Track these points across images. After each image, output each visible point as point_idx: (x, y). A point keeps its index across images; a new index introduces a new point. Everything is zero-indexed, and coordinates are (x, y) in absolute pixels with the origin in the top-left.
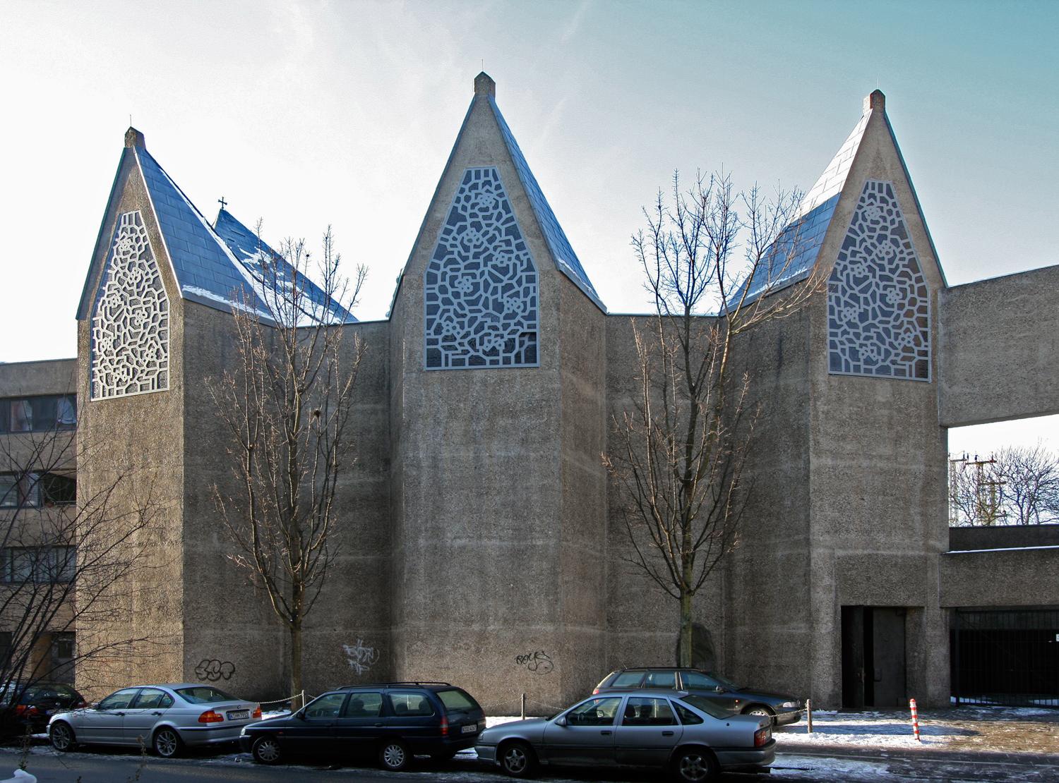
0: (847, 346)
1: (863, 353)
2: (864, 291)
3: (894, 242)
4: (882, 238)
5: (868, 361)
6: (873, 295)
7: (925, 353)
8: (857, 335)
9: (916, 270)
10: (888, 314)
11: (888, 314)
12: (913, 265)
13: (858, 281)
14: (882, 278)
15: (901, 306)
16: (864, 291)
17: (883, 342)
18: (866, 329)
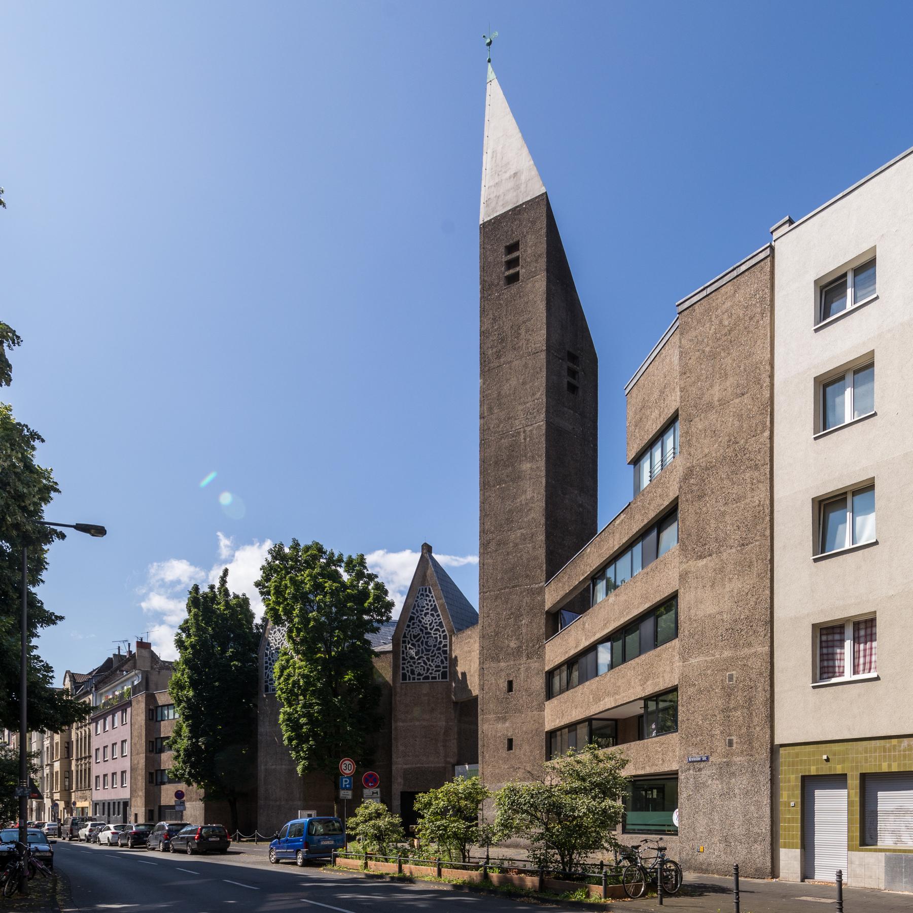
0: (410, 668)
1: (417, 671)
2: (418, 641)
3: (432, 615)
4: (426, 614)
5: (419, 674)
6: (422, 643)
7: (446, 667)
8: (414, 663)
9: (442, 627)
10: (429, 651)
11: (429, 651)
12: (441, 624)
13: (415, 637)
14: (426, 633)
15: (435, 646)
16: (418, 641)
17: (426, 664)
18: (418, 659)
